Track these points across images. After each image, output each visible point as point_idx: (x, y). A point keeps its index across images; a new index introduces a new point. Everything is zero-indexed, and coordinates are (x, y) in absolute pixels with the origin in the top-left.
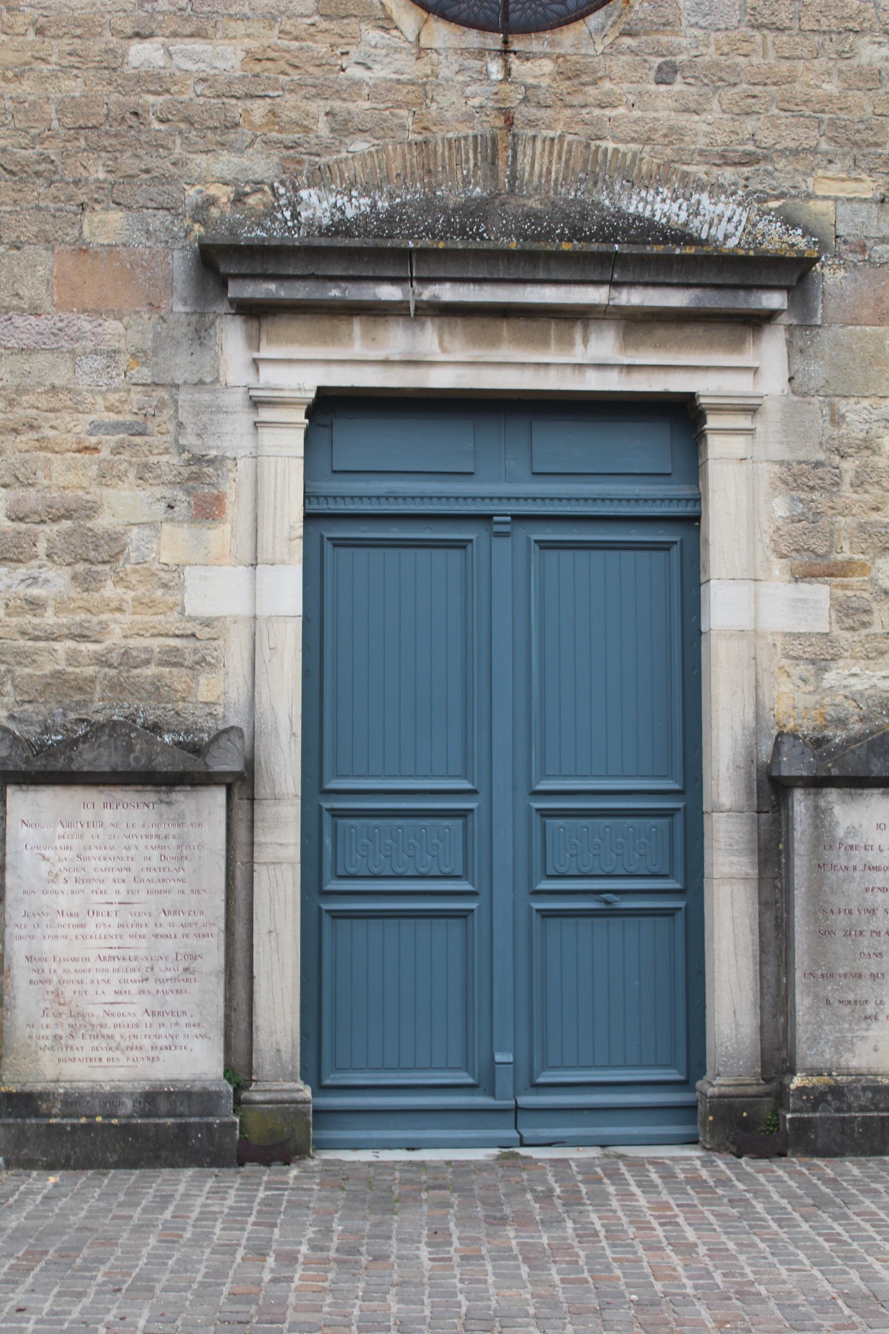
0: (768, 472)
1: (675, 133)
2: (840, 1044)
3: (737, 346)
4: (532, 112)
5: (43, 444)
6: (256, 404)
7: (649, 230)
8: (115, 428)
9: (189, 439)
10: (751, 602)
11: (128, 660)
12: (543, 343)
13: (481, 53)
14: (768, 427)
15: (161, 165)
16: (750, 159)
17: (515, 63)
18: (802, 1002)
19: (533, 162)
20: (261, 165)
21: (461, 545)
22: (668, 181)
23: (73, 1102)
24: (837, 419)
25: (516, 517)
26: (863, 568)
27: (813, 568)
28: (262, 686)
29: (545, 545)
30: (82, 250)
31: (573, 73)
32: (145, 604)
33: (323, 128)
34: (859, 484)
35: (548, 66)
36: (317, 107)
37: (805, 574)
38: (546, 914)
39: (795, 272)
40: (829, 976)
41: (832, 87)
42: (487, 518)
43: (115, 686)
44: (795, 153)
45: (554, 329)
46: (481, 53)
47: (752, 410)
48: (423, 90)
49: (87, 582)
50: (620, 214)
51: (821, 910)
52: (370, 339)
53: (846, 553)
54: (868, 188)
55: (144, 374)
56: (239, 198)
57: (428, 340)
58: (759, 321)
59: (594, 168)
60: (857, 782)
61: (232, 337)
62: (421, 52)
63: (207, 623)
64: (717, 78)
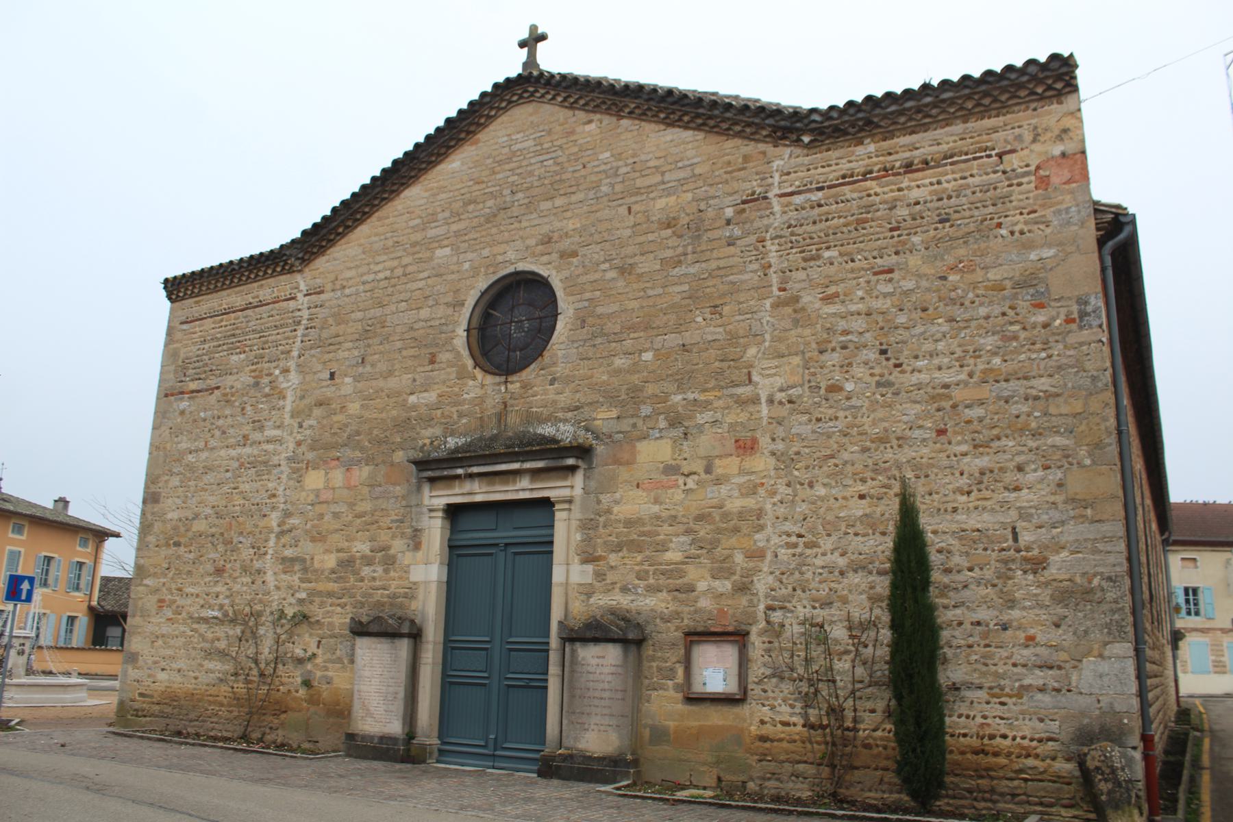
0: (574, 524)
1: (555, 402)
2: (576, 739)
3: (565, 478)
4: (512, 402)
5: (379, 528)
6: (431, 511)
7: (544, 439)
8: (397, 521)
9: (414, 524)
11: (395, 596)
12: (514, 482)
13: (499, 384)
14: (576, 507)
15: (413, 435)
16: (577, 408)
17: (509, 386)
18: (565, 722)
19: (513, 420)
20: (437, 431)
21: (491, 554)
22: (550, 420)
23: (364, 737)
24: (599, 502)
25: (507, 545)
26: (604, 558)
27: (588, 559)
28: (429, 607)
29: (516, 554)
30: (392, 465)
32: (400, 578)
33: (455, 416)
34: (605, 527)
35: (518, 385)
36: (454, 409)
37: (585, 561)
38: (509, 686)
40: (574, 713)
41: (605, 378)
42: (497, 545)
43: (391, 604)
44: (591, 403)
45: (511, 478)
46: (499, 384)
47: (570, 502)
48: (481, 400)
49: (386, 571)
50: (535, 434)
51: (572, 688)
52: (460, 487)
53: (600, 552)
54: (614, 414)
55: (404, 503)
56: (432, 443)
57: (475, 486)
58: (573, 469)
59: (530, 418)
60: (585, 640)
61: (426, 489)
62: (483, 386)
63: (415, 583)
64: (568, 380)
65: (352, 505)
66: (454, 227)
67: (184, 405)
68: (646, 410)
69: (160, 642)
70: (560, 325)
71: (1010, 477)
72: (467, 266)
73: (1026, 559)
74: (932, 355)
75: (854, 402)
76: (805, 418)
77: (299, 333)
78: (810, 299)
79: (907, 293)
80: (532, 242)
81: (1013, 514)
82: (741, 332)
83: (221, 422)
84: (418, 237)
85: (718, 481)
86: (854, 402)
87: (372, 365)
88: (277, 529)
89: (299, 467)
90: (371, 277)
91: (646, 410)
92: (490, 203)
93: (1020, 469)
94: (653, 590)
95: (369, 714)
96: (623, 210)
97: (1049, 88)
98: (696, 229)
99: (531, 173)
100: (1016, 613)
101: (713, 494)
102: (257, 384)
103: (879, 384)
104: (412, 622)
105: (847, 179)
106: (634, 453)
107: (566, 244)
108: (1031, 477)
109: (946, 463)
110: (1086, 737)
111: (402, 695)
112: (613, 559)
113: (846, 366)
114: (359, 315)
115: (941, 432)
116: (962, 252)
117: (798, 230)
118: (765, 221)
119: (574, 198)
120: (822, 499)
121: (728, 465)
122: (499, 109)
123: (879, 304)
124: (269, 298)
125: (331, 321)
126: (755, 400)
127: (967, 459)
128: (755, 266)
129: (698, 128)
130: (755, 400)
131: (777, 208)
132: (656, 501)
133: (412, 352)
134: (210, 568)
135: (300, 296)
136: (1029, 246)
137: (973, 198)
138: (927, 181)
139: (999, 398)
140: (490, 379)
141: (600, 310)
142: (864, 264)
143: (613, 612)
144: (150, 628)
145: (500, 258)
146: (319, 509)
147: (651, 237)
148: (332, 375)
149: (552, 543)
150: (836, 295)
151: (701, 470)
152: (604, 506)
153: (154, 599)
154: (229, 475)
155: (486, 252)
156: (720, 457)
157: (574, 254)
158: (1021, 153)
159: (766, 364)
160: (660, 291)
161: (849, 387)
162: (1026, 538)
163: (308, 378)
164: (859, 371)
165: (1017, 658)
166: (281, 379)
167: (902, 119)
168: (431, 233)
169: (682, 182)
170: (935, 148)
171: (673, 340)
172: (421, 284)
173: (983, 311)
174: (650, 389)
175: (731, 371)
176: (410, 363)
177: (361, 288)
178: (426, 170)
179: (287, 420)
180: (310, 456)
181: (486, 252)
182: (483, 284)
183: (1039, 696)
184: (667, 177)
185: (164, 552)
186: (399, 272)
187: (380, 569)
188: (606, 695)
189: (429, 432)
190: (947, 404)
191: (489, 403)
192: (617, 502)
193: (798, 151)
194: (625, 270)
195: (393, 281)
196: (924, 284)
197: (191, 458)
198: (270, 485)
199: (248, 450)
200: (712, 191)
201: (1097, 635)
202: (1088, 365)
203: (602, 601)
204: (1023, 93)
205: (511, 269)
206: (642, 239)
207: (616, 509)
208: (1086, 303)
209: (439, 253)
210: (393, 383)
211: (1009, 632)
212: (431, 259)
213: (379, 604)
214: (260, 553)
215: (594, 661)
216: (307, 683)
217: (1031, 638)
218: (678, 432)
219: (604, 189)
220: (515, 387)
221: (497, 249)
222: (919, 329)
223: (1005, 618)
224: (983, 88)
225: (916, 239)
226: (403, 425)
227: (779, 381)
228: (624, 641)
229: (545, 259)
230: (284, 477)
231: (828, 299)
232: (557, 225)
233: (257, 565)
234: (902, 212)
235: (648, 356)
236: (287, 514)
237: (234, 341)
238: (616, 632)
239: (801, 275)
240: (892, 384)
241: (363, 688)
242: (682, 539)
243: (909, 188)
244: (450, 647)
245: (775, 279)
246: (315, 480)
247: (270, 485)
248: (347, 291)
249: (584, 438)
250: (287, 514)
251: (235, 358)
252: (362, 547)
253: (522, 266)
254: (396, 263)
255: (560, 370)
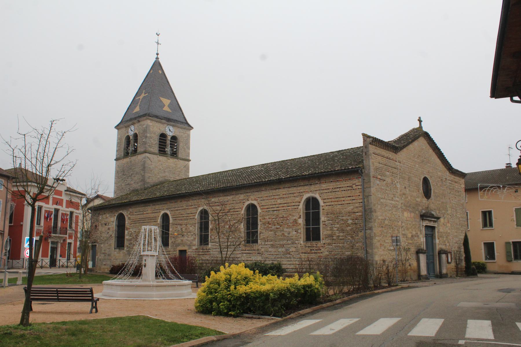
124: (392, 158)
153: (379, 243)
185: (381, 229)
197: (382, 200)
199: (393, 202)
216: (410, 265)
250: (402, 222)
252: (414, 233)
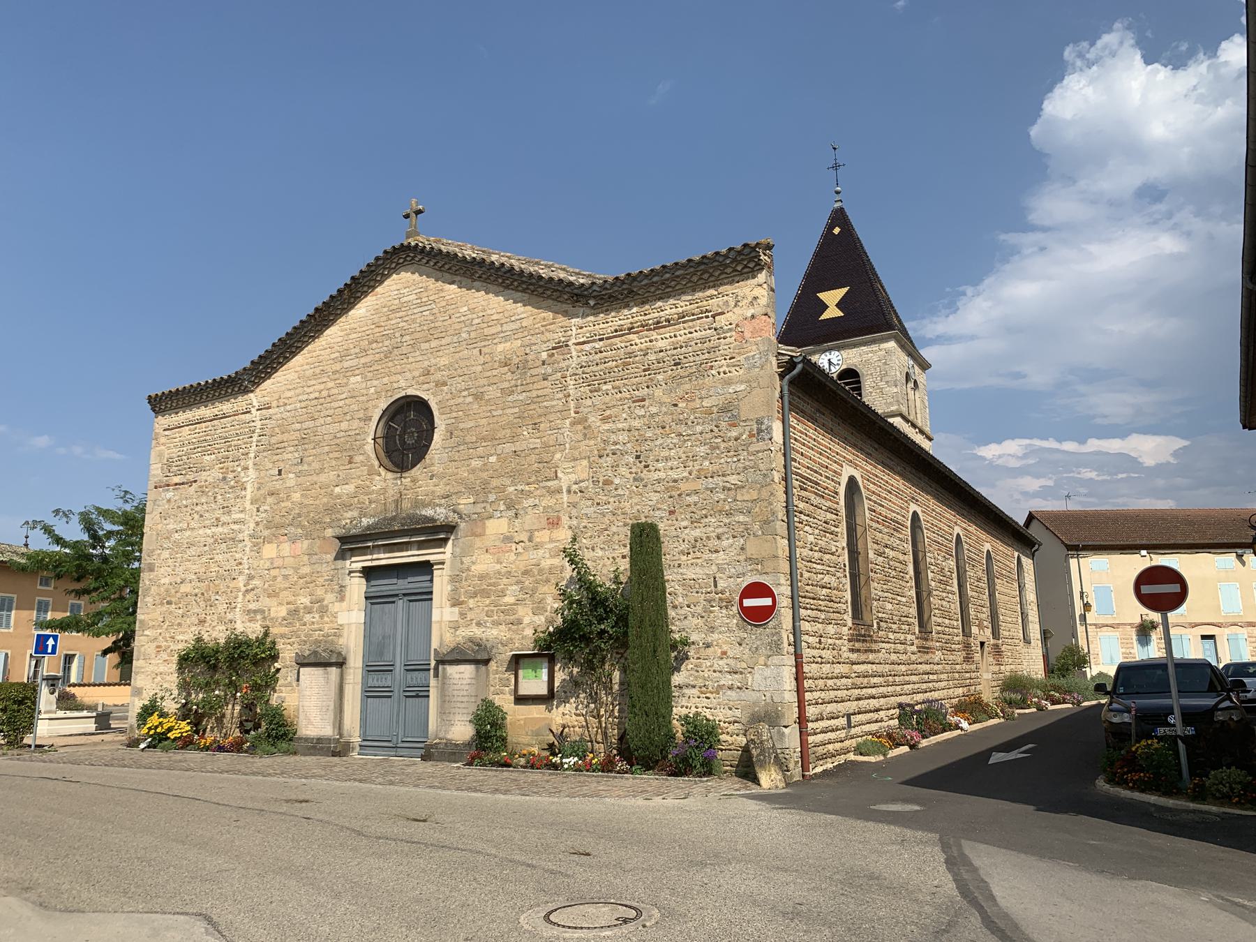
0: (446, 579)
10: (442, 612)
16: (448, 496)
19: (406, 505)
20: (355, 514)
24: (462, 563)
27: (456, 603)
30: (324, 538)
31: (414, 481)
37: (453, 605)
39: (450, 528)
42: (397, 595)
48: (385, 490)
49: (322, 617)
53: (463, 598)
54: (472, 500)
58: (446, 540)
59: (418, 504)
65: (296, 569)
66: (363, 360)
67: (170, 495)
68: (492, 497)
69: (159, 678)
70: (436, 436)
71: (714, 543)
72: (372, 390)
73: (721, 599)
74: (667, 459)
75: (620, 492)
76: (590, 503)
77: (254, 439)
78: (594, 420)
79: (652, 416)
80: (416, 373)
81: (714, 567)
82: (551, 443)
83: (199, 508)
84: (337, 367)
85: (536, 547)
86: (620, 492)
87: (309, 465)
88: (243, 589)
89: (258, 542)
90: (306, 397)
91: (492, 497)
92: (387, 343)
93: (719, 538)
94: (497, 624)
95: (310, 722)
96: (476, 352)
97: (746, 266)
98: (521, 367)
99: (414, 321)
100: (715, 636)
101: (534, 555)
102: (224, 478)
103: (635, 480)
104: (340, 654)
105: (619, 332)
106: (484, 528)
107: (438, 376)
108: (725, 543)
109: (675, 533)
110: (756, 719)
111: (332, 707)
112: (471, 603)
113: (615, 467)
114: (298, 426)
115: (671, 513)
116: (687, 386)
117: (586, 370)
118: (567, 363)
119: (444, 342)
120: (601, 558)
121: (542, 536)
122: (390, 268)
123: (636, 423)
125: (277, 430)
126: (559, 491)
127: (687, 531)
128: (560, 395)
129: (524, 291)
130: (559, 491)
131: (574, 354)
132: (499, 562)
133: (337, 455)
134: (195, 620)
135: (253, 410)
136: (729, 383)
137: (696, 348)
138: (667, 335)
139: (707, 489)
140: (390, 475)
141: (461, 426)
142: (627, 395)
143: (471, 640)
144: (151, 668)
145: (395, 385)
146: (273, 572)
147: (495, 373)
148: (280, 471)
149: (431, 593)
150: (609, 417)
151: (526, 540)
152: (465, 566)
154: (206, 548)
155: (386, 380)
156: (537, 530)
157: (445, 384)
158: (727, 315)
159: (567, 465)
160: (500, 412)
161: (617, 481)
162: (722, 584)
163: (263, 474)
164: (623, 470)
165: (716, 667)
166: (242, 474)
167: (653, 289)
168: (346, 364)
169: (515, 331)
170: (674, 310)
171: (509, 448)
172: (341, 403)
173: (699, 429)
174: (495, 483)
175: (545, 472)
176: (334, 463)
177: (298, 405)
178: (340, 315)
179: (248, 505)
180: (266, 533)
181: (386, 380)
182: (384, 405)
183: (729, 692)
184: (505, 327)
186: (325, 393)
187: (317, 616)
188: (465, 699)
189: (349, 514)
190: (675, 493)
191: (390, 492)
192: (473, 563)
193: (588, 311)
194: (478, 397)
195: (322, 401)
196: (664, 409)
198: (237, 556)
199: (220, 529)
200: (534, 340)
201: (763, 651)
202: (762, 466)
203: (464, 633)
204: (729, 270)
205: (403, 394)
206: (489, 374)
207: (473, 568)
208: (762, 423)
209: (353, 380)
210: (323, 478)
211: (711, 649)
212: (347, 384)
213: (317, 642)
214: (231, 606)
215: (457, 676)
217: (724, 653)
218: (511, 513)
219: (464, 335)
220: (407, 481)
221: (394, 378)
222: (658, 443)
223: (709, 640)
224: (703, 267)
225: (660, 377)
226: (330, 510)
227: (573, 477)
228: (476, 662)
229: (426, 386)
230: (247, 549)
231: (605, 420)
232: (433, 361)
233: (229, 616)
234: (652, 357)
235: (493, 459)
236: (251, 577)
237: (204, 446)
238: (471, 656)
239: (589, 402)
240: (642, 480)
241: (306, 704)
242: (514, 587)
243: (656, 340)
244: (369, 669)
245: (572, 405)
246: (269, 551)
247: (237, 556)
248: (288, 408)
249: (453, 518)
250: (251, 577)
251: (207, 458)
252: (304, 600)
253: (411, 392)
254: (322, 387)
255: (437, 469)
